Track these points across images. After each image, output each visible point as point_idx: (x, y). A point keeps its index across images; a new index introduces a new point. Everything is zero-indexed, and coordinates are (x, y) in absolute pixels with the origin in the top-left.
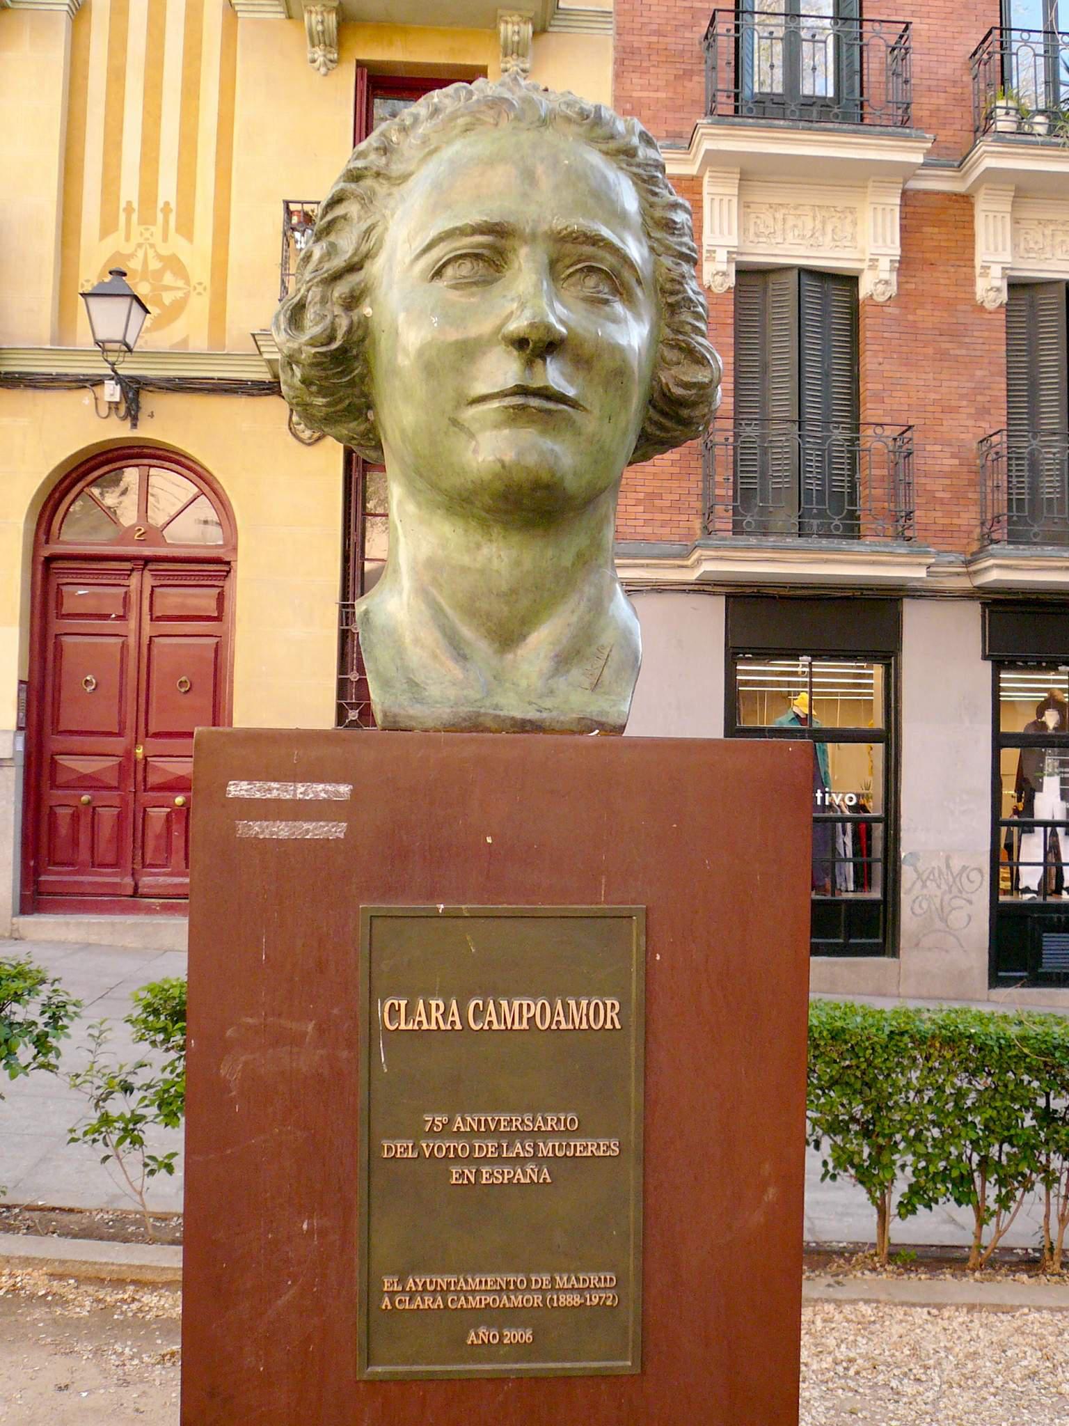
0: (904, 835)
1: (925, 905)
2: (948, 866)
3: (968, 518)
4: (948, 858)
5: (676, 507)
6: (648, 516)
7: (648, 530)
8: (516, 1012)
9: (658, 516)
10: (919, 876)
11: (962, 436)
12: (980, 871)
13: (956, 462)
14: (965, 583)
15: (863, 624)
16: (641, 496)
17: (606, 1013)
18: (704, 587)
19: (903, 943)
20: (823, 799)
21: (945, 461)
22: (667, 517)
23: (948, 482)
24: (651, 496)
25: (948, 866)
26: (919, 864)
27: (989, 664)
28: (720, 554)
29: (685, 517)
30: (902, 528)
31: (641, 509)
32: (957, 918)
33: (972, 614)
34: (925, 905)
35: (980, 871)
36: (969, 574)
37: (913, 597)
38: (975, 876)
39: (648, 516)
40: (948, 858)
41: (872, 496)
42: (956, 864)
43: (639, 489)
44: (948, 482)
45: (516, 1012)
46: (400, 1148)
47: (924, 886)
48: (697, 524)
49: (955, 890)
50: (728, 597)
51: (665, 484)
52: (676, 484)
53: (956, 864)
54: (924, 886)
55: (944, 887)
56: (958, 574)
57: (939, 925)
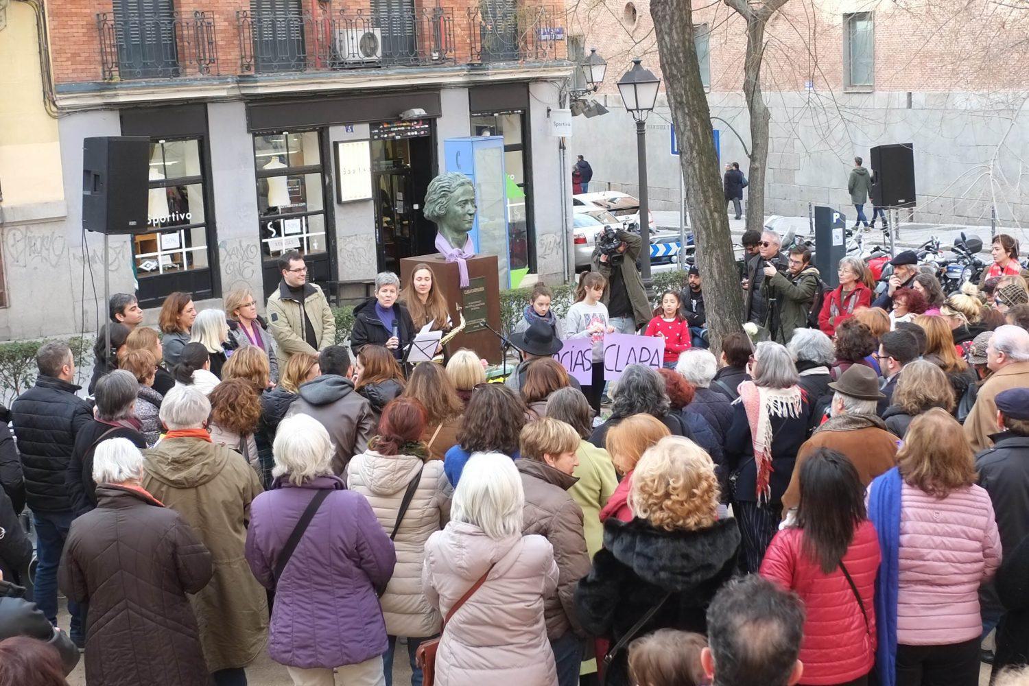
0: (219, 232)
1: (232, 268)
2: (241, 246)
3: (234, 55)
4: (240, 242)
5: (88, 61)
6: (74, 67)
7: (75, 75)
8: (476, 290)
9: (79, 67)
10: (228, 253)
11: (228, 9)
12: (256, 246)
13: (227, 23)
14: (236, 92)
15: (189, 120)
16: (69, 55)
17: (482, 289)
18: (109, 107)
19: (223, 290)
20: (176, 217)
21: (222, 24)
22: (84, 67)
23: (223, 35)
24: (75, 55)
25: (241, 246)
26: (227, 248)
27: (251, 136)
28: (129, 92)
29: (93, 66)
30: (207, 65)
31: (70, 63)
32: (247, 273)
33: (240, 108)
34: (232, 268)
35: (256, 246)
36: (239, 87)
37: (213, 102)
38: (253, 249)
39: (74, 67)
40: (240, 242)
41: (187, 47)
42: (244, 244)
43: (67, 51)
44: (223, 35)
45: (476, 290)
46: (467, 307)
47: (231, 258)
48: (100, 69)
49: (245, 259)
50: (120, 110)
51: (82, 47)
52: (86, 47)
53: (244, 244)
54: (231, 258)
55: (240, 257)
56: (233, 88)
57: (239, 277)
